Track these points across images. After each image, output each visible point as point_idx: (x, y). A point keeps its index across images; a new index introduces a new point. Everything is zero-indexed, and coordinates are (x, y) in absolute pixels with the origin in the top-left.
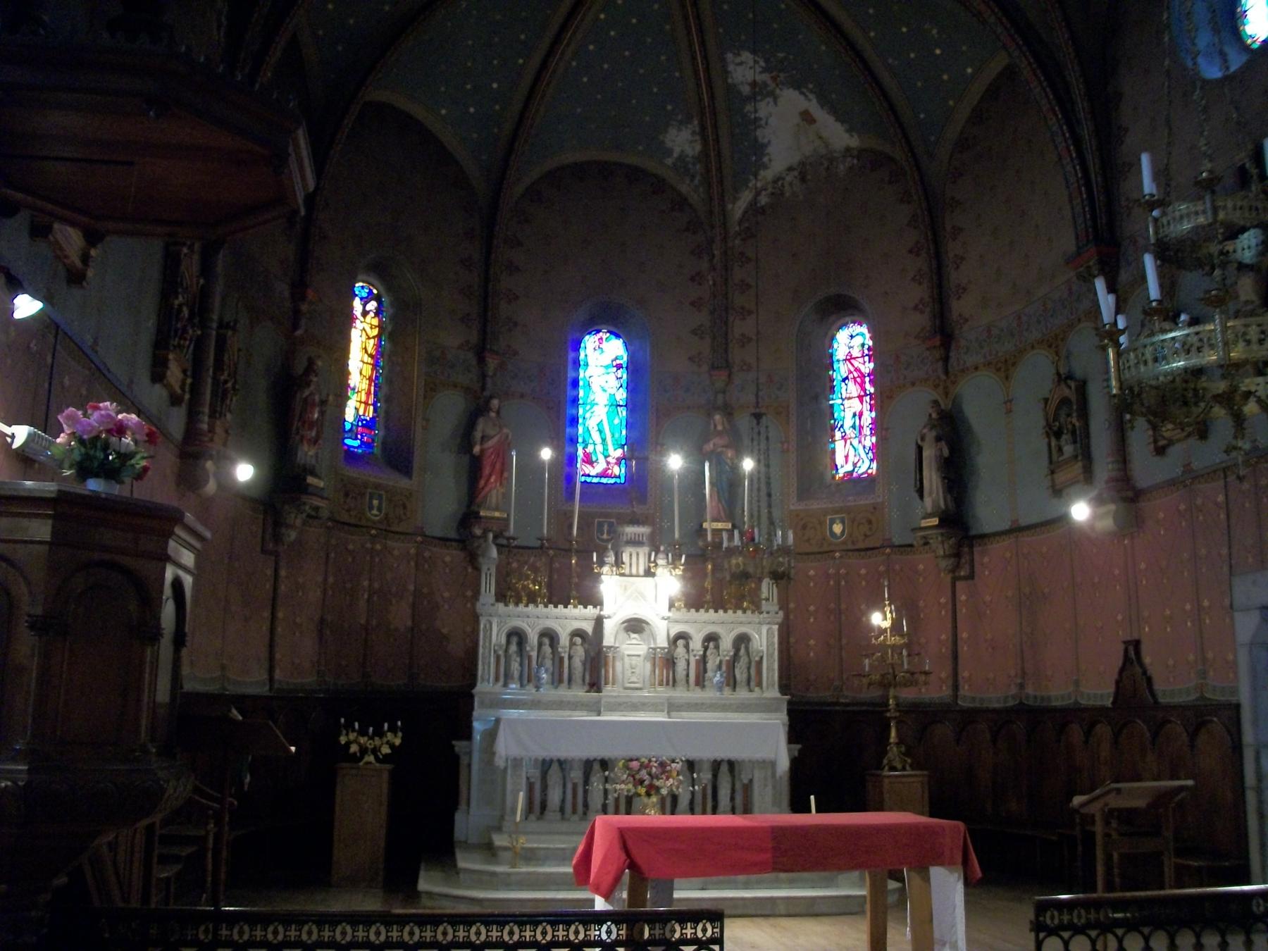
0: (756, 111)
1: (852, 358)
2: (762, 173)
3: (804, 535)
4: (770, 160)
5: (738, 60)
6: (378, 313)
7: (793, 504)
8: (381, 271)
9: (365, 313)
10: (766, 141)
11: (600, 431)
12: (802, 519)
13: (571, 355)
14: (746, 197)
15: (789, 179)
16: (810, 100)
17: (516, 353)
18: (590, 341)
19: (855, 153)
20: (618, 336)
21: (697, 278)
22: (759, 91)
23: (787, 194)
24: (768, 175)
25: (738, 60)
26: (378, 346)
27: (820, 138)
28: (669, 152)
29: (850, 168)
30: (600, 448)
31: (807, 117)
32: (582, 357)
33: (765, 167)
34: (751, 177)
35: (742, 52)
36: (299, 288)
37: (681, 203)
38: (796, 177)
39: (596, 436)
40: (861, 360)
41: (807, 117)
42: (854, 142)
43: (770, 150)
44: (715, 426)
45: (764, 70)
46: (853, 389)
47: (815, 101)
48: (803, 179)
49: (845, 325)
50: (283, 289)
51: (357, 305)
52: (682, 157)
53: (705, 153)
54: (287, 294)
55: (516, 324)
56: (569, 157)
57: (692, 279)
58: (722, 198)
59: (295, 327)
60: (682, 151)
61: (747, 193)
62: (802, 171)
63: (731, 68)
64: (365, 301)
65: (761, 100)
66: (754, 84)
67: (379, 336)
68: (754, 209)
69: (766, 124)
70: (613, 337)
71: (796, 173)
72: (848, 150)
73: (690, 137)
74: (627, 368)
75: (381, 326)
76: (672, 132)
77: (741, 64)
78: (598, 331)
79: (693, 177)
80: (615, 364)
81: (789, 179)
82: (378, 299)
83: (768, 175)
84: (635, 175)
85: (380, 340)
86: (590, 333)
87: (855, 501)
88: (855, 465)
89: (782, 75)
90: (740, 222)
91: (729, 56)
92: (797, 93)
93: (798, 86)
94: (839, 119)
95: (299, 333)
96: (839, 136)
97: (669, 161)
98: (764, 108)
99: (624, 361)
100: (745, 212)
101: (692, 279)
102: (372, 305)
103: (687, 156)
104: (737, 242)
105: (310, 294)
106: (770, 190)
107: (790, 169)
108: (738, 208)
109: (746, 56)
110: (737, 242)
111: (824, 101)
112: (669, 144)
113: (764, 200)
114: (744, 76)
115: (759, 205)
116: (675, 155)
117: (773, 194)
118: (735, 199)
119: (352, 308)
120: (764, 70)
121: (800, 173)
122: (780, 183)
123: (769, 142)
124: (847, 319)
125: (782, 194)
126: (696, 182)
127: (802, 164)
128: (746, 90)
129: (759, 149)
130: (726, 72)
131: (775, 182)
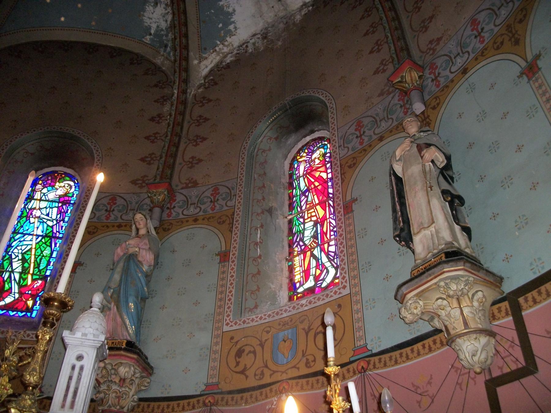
1: (312, 171)
3: (238, 363)
4: (236, 28)
7: (227, 324)
10: (230, 10)
11: (24, 260)
12: (237, 342)
30: (17, 276)
33: (230, 34)
39: (17, 265)
40: (323, 169)
43: (234, 18)
44: (138, 230)
46: (313, 198)
52: (158, 34)
60: (158, 27)
61: (214, 55)
73: (164, 11)
79: (166, 46)
80: (62, 199)
83: (235, 41)
87: (310, 303)
88: (316, 278)
90: (206, 77)
112: (147, 22)
123: (234, 10)
126: (168, 49)
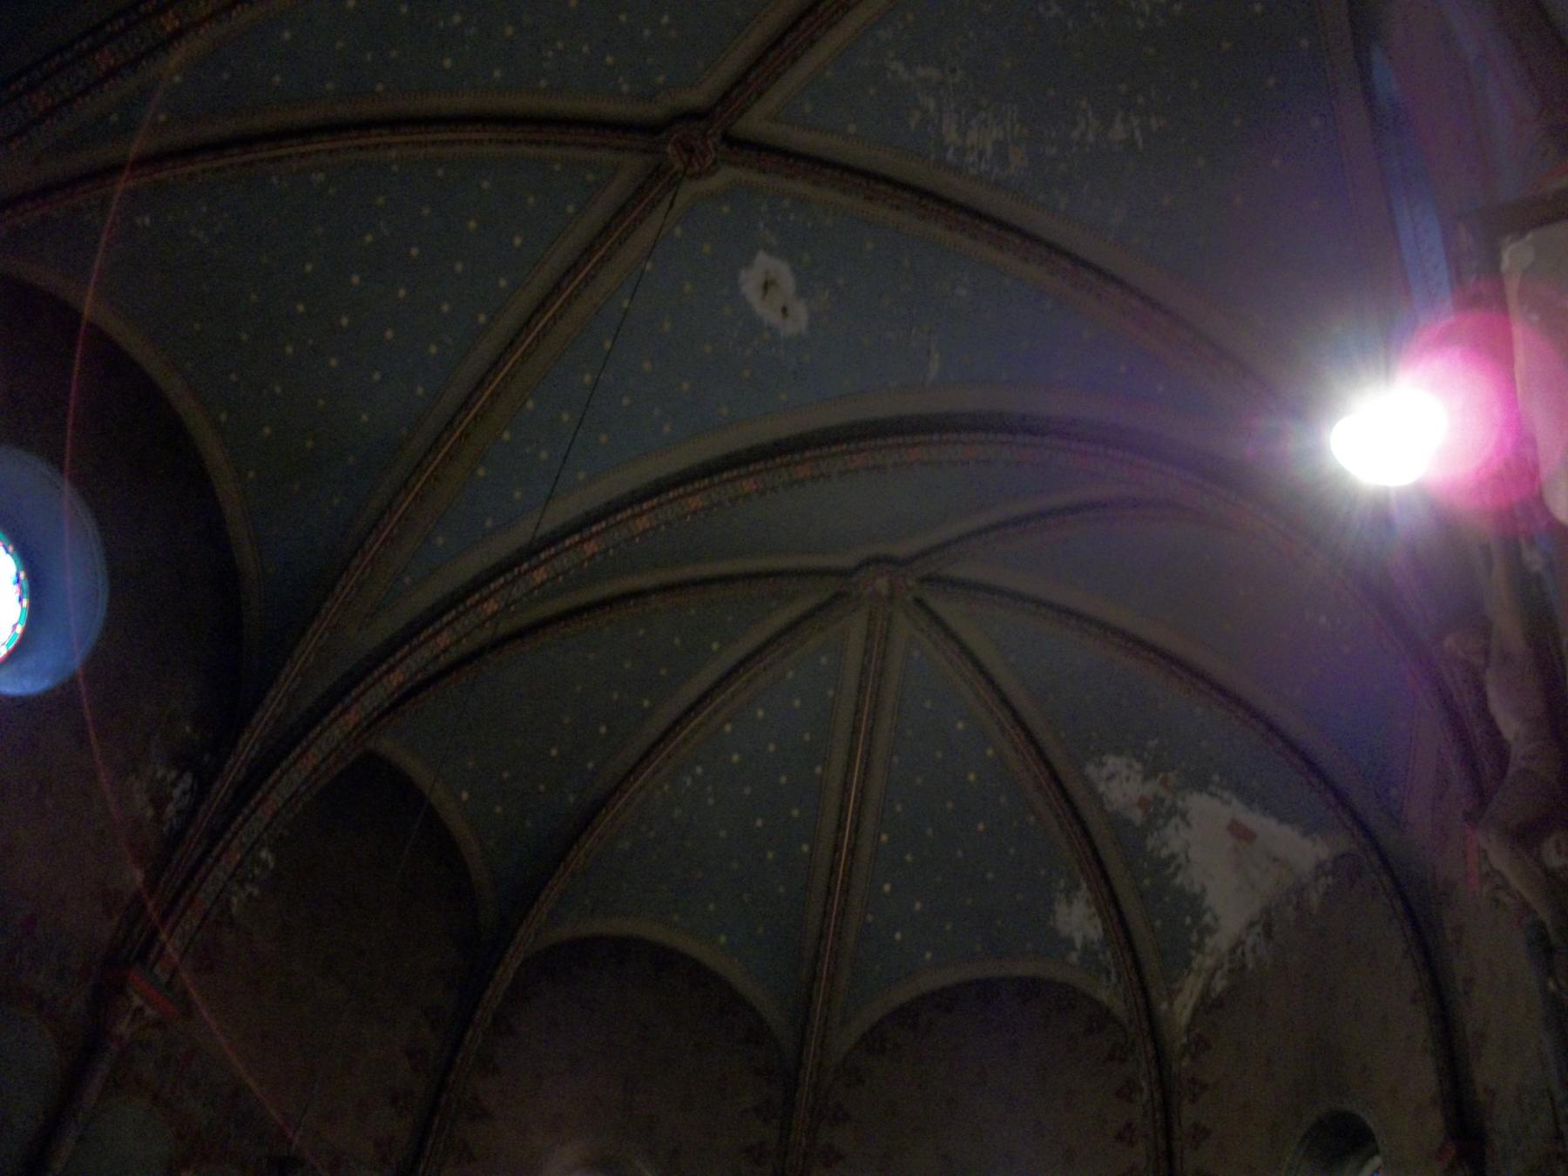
0: (1166, 844)
2: (1210, 942)
5: (1105, 773)
15: (1250, 941)
16: (1228, 803)
19: (1329, 865)
21: (1125, 1135)
23: (1250, 966)
24: (1220, 941)
25: (1105, 773)
27: (1275, 860)
28: (1068, 943)
29: (1326, 894)
31: (1241, 833)
33: (1208, 930)
34: (1193, 953)
35: (1104, 759)
38: (1259, 935)
41: (1241, 833)
45: (1146, 778)
47: (1235, 802)
48: (1268, 933)
57: (1120, 1137)
60: (1084, 937)
62: (1266, 924)
63: (1102, 788)
65: (1165, 825)
66: (1142, 803)
68: (1209, 1005)
69: (1188, 861)
71: (1258, 929)
76: (1061, 909)
77: (1111, 777)
79: (1108, 973)
81: (1250, 941)
83: (1220, 941)
84: (1030, 988)
89: (1172, 776)
90: (1188, 1030)
91: (1090, 770)
92: (1205, 797)
94: (1282, 820)
97: (1074, 957)
100: (1195, 1011)
101: (1120, 1137)
103: (1092, 943)
104: (1186, 1062)
106: (1227, 966)
107: (1252, 924)
109: (1112, 762)
110: (1186, 1062)
111: (1249, 798)
113: (1220, 984)
114: (1125, 795)
115: (1213, 995)
116: (1078, 945)
117: (1231, 971)
118: (1172, 995)
120: (1146, 778)
122: (1239, 951)
123: (1204, 890)
125: (1244, 967)
127: (1266, 911)
128: (1137, 816)
129: (1193, 904)
131: (1233, 951)
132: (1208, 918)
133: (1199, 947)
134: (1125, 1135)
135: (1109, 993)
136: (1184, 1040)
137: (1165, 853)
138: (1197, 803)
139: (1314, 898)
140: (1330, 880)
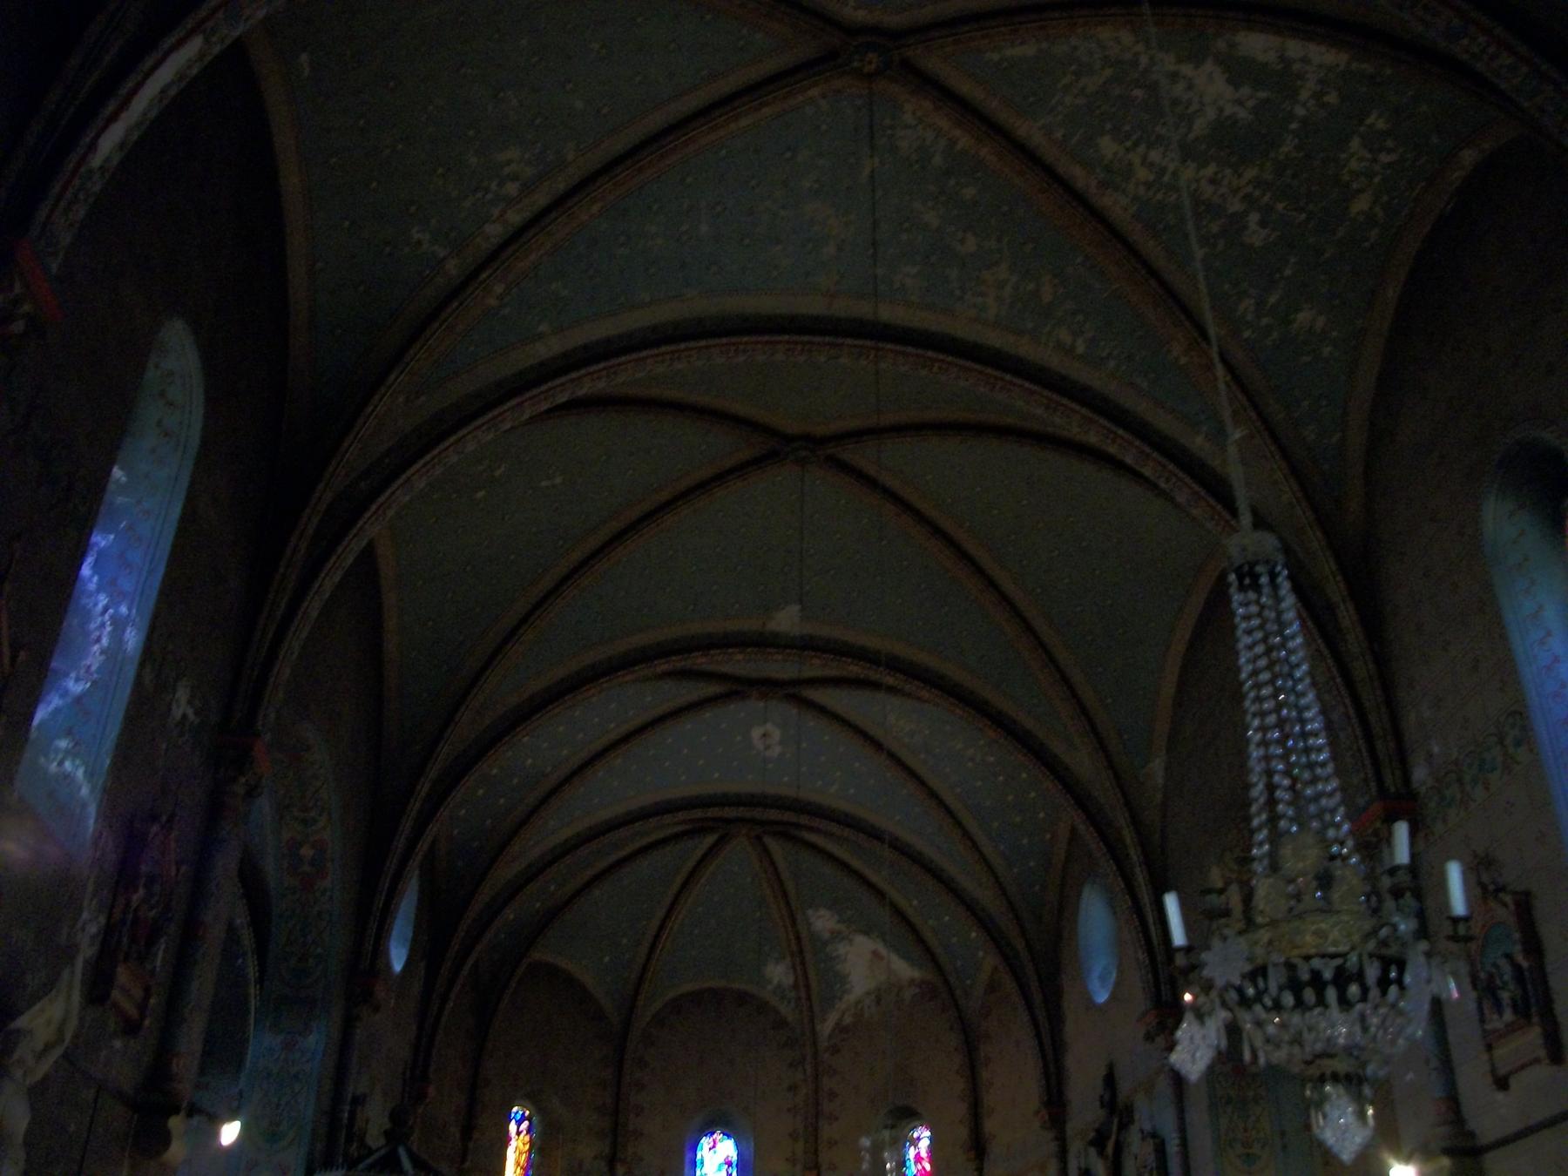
6: (529, 1131)
8: (533, 1099)
9: (518, 1133)
13: (688, 1156)
14: (832, 1018)
17: (641, 1159)
18: (705, 1142)
20: (729, 1137)
21: (793, 1088)
22: (836, 936)
24: (851, 998)
26: (529, 1158)
32: (699, 1157)
36: (468, 1130)
37: (781, 1023)
41: (875, 953)
42: (916, 974)
45: (839, 922)
48: (878, 1001)
49: (916, 1127)
50: (455, 1131)
51: (513, 1127)
52: (779, 986)
53: (795, 986)
54: (458, 1135)
55: (642, 1134)
56: (687, 988)
58: (812, 1021)
59: (463, 1160)
62: (878, 996)
64: (519, 1123)
67: (530, 1151)
68: (840, 1029)
70: (725, 1137)
71: (873, 997)
72: (912, 982)
74: (737, 1165)
75: (531, 1141)
77: (820, 917)
78: (713, 1133)
82: (529, 1119)
83: (851, 998)
84: (743, 998)
85: (530, 1155)
86: (706, 1136)
90: (830, 1037)
91: (810, 912)
93: (867, 933)
95: (467, 1164)
96: (904, 970)
97: (770, 987)
98: (842, 949)
99: (734, 1158)
102: (525, 1125)
105: (476, 1135)
107: (868, 993)
108: (826, 1028)
109: (822, 912)
113: (848, 1020)
118: (824, 1020)
119: (508, 1131)
120: (839, 922)
121: (876, 996)
124: (917, 1123)
129: (843, 979)
130: (809, 924)
132: (848, 986)
133: (840, 999)
134: (793, 1088)
135: (786, 1010)
136: (826, 1044)
137: (834, 954)
138: (860, 939)
139: (908, 994)
140: (917, 990)
